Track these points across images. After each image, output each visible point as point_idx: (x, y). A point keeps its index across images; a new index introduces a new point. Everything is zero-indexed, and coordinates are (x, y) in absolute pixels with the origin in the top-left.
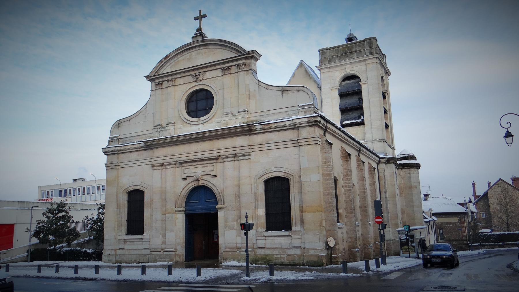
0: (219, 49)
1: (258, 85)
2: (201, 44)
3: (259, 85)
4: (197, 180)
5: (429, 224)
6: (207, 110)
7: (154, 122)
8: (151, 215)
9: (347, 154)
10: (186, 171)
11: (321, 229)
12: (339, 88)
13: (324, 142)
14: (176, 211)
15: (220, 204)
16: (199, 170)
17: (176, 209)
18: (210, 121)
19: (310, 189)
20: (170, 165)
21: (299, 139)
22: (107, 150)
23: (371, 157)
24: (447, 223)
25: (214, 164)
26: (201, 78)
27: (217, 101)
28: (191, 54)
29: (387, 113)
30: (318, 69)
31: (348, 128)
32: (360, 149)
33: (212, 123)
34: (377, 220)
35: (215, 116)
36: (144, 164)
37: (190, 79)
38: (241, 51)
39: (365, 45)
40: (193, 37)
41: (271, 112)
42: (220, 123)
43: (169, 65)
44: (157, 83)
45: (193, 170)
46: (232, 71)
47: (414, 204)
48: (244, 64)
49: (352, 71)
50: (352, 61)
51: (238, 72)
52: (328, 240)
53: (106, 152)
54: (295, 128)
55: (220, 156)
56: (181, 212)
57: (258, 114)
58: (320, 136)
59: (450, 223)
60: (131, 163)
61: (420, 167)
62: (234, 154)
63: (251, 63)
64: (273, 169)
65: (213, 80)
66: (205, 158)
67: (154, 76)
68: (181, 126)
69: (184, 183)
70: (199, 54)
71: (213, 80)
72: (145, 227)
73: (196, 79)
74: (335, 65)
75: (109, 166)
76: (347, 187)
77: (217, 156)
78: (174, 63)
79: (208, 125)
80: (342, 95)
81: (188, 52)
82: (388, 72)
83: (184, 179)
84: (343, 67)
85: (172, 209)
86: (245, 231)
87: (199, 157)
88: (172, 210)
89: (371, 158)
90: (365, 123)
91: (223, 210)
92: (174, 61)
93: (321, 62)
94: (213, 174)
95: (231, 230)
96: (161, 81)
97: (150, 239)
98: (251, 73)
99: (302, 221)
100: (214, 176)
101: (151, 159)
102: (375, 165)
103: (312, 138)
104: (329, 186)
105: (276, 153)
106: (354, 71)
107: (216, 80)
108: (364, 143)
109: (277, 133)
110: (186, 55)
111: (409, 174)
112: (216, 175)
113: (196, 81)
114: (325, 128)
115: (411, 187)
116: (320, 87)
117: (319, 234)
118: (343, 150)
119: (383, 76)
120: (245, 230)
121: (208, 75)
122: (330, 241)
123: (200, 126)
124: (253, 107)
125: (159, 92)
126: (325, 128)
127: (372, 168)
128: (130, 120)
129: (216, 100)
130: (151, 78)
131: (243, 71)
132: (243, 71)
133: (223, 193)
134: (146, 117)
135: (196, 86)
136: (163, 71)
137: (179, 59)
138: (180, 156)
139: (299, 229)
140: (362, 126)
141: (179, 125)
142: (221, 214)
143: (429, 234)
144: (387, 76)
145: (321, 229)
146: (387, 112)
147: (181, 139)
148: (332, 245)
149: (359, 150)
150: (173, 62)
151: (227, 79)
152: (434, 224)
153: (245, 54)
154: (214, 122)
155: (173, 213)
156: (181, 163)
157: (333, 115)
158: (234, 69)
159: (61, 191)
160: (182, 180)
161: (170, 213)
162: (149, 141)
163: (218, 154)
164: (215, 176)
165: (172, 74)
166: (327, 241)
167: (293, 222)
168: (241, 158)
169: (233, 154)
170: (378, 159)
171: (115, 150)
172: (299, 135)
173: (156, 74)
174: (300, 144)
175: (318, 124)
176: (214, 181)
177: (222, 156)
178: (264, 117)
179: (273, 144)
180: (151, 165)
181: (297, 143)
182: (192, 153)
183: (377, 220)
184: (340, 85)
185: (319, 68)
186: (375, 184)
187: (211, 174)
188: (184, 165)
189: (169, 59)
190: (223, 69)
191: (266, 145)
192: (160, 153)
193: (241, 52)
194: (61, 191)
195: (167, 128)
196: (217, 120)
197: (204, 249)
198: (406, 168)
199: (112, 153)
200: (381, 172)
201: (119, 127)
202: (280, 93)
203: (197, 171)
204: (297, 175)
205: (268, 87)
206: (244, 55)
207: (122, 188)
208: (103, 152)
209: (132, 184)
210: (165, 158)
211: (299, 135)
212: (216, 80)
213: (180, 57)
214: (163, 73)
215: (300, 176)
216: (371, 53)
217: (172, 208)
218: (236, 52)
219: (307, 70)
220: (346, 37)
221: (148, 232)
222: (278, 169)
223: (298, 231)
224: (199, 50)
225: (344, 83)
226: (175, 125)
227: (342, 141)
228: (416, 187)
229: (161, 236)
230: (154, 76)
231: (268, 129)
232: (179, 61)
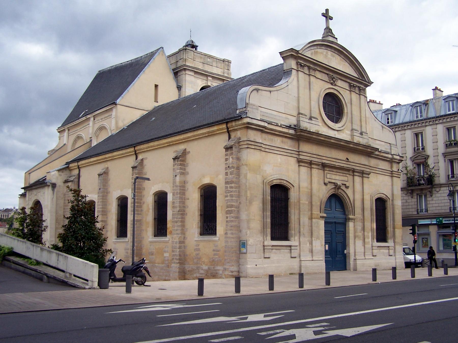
0: (347, 63)
2: (341, 49)
10: (328, 176)
15: (351, 215)
16: (338, 177)
25: (348, 175)
37: (326, 78)
45: (333, 177)
65: (343, 91)
66: (346, 167)
70: (333, 56)
73: (332, 81)
78: (313, 51)
85: (318, 214)
91: (353, 221)
112: (349, 187)
121: (339, 83)
123: (336, 132)
142: (351, 225)
153: (367, 81)
174: (394, 175)
177: (356, 169)
192: (306, 148)
202: (381, 128)
206: (367, 82)
209: (277, 176)
224: (334, 52)
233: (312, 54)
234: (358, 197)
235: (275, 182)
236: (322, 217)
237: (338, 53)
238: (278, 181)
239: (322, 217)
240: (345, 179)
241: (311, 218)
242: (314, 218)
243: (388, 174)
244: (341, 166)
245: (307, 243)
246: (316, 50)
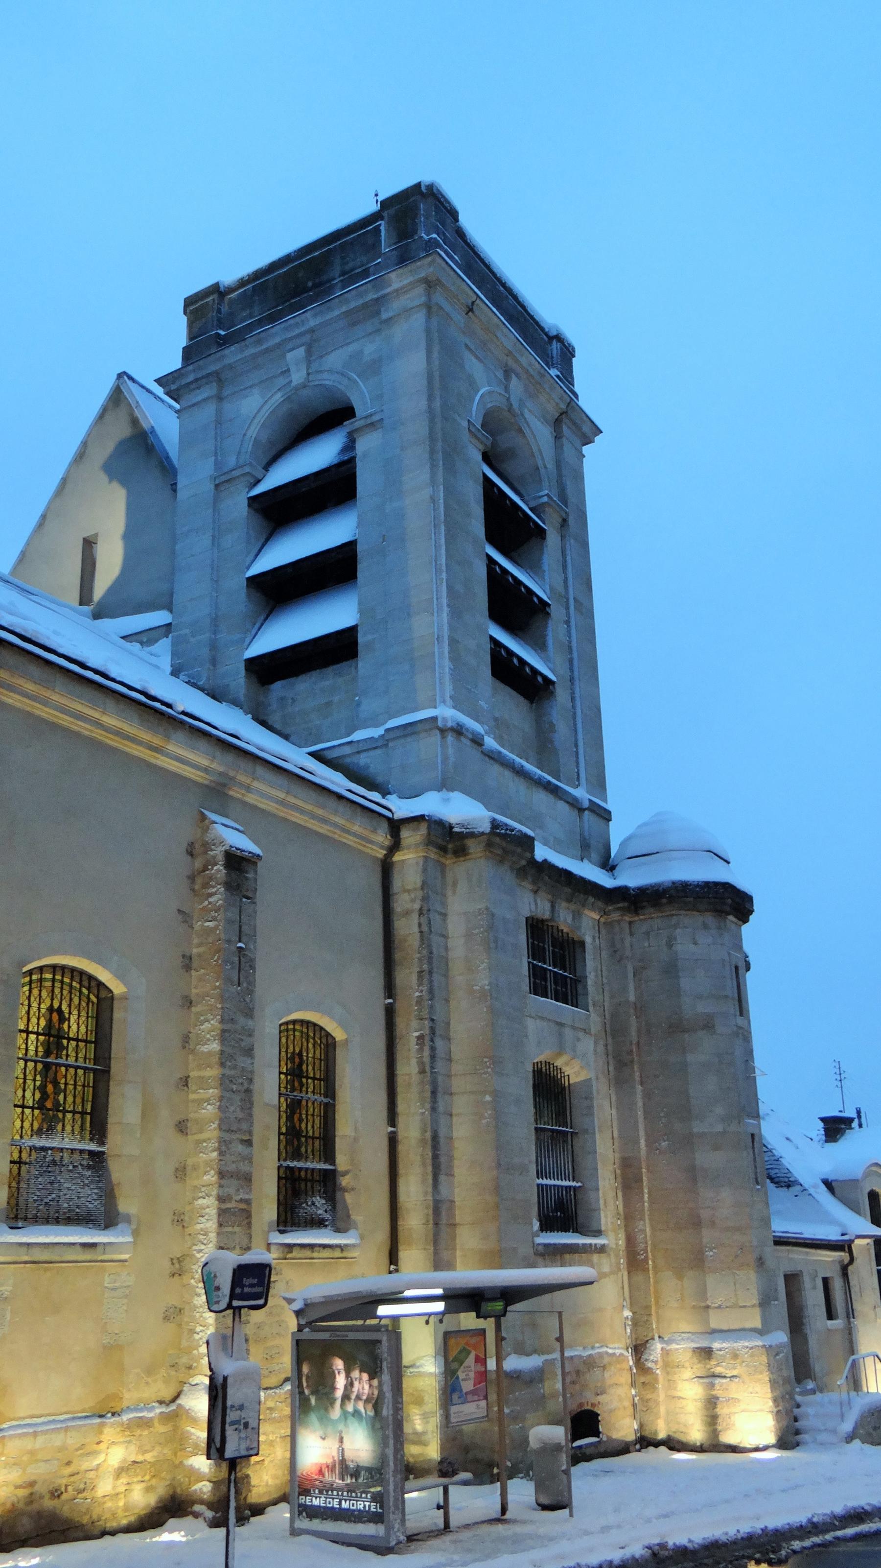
31: (292, 680)
47: (698, 1127)
108: (347, 750)
111: (670, 946)
185: (173, 387)
200: (407, 913)
219: (137, 413)
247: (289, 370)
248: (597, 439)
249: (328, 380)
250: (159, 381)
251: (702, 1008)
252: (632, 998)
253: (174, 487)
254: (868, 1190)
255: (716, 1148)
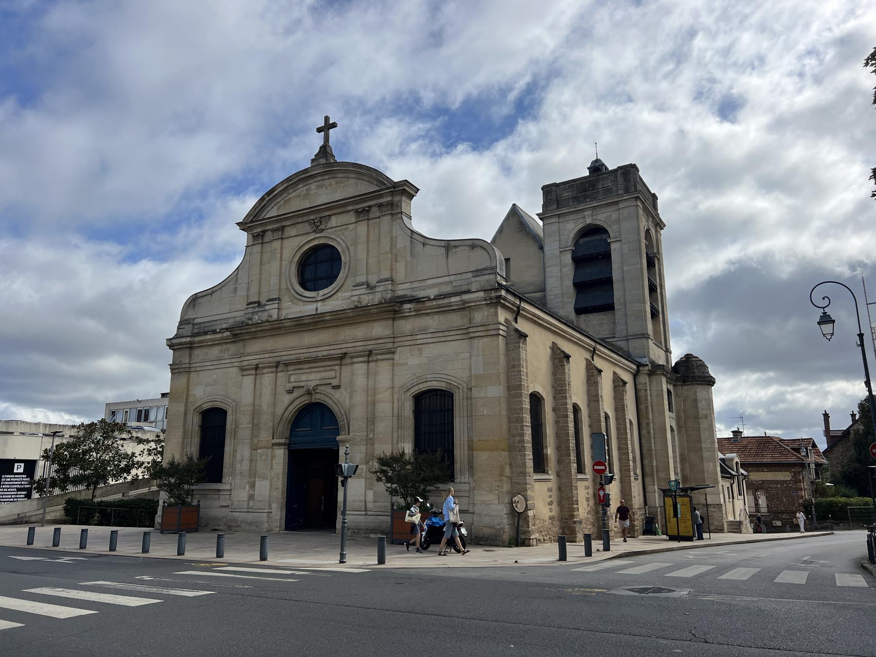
1: (410, 239)
3: (411, 238)
4: (309, 393)
5: (732, 482)
6: (331, 278)
7: (248, 296)
8: (235, 451)
9: (562, 355)
11: (501, 480)
12: (574, 249)
13: (512, 333)
14: (273, 445)
15: (343, 433)
16: (312, 376)
17: (274, 441)
18: (335, 296)
19: (485, 411)
20: (269, 367)
21: (470, 326)
22: (174, 341)
23: (619, 362)
24: (772, 482)
25: (337, 368)
26: (322, 227)
27: (345, 263)
28: (310, 187)
29: (657, 292)
30: (540, 219)
31: (588, 315)
32: (594, 349)
33: (337, 299)
34: (596, 467)
35: (343, 289)
36: (229, 365)
38: (385, 182)
39: (618, 176)
40: (313, 160)
41: (429, 282)
42: (349, 300)
43: (275, 205)
44: (255, 235)
45: (304, 377)
46: (371, 215)
48: (391, 204)
49: (596, 221)
50: (594, 205)
51: (379, 217)
52: (513, 501)
53: (171, 344)
54: (464, 308)
55: (346, 354)
56: (281, 447)
57: (407, 286)
58: (505, 322)
59: (777, 482)
60: (209, 363)
61: (714, 383)
62: (367, 351)
63: (400, 201)
64: (428, 376)
65: (341, 230)
66: (322, 356)
67: (251, 222)
68: (290, 305)
69: (287, 399)
70: (322, 187)
71: (341, 230)
72: (225, 470)
74: (567, 211)
75: (176, 369)
76: (562, 410)
77: (342, 354)
78: (282, 202)
79: (330, 302)
80: (579, 261)
81: (305, 184)
82: (659, 223)
83: (290, 392)
84: (581, 215)
85: (268, 441)
86: (343, 479)
87: (314, 355)
88: (268, 442)
89: (620, 364)
90: (616, 307)
92: (283, 199)
93: (545, 206)
94: (335, 382)
95: (358, 478)
96: (262, 232)
97: (230, 490)
98: (400, 218)
99: (471, 466)
100: (336, 386)
101: (240, 357)
102: (627, 377)
103: (490, 326)
104: (518, 407)
105: (432, 351)
106: (598, 221)
107: (345, 229)
109: (436, 317)
110: (302, 189)
113: (314, 231)
114: (515, 309)
115: (698, 415)
116: (543, 248)
117: (497, 490)
118: (554, 348)
119: (650, 229)
120: (342, 475)
122: (518, 502)
123: (319, 304)
124: (400, 274)
125: (258, 248)
126: (515, 309)
127: (620, 381)
128: (211, 295)
129: (344, 262)
130: (247, 226)
131: (387, 214)
132: (387, 214)
133: (348, 415)
134: (236, 288)
135: (314, 239)
136: (265, 215)
137: (292, 195)
138: (284, 353)
139: (466, 480)
140: (610, 312)
141: (286, 303)
143: (733, 498)
144: (658, 229)
145: (501, 480)
146: (657, 289)
147: (286, 324)
148: (520, 508)
149: (592, 349)
150: (281, 201)
151: (362, 228)
152: (744, 481)
154: (340, 299)
155: (268, 448)
156: (286, 365)
157: (562, 293)
158: (375, 212)
159: (140, 412)
160: (285, 393)
161: (265, 447)
162: (237, 329)
163: (343, 351)
164: (337, 387)
165: (279, 219)
166: (512, 502)
167: (457, 466)
168: (379, 357)
169: (366, 351)
170: (635, 367)
171: (185, 342)
172: (470, 320)
173: (254, 219)
174: (472, 335)
175: (502, 301)
176: (337, 394)
178: (417, 291)
179: (430, 335)
180: (239, 367)
181: (467, 333)
182: (303, 349)
183: (596, 467)
184: (576, 243)
185: (542, 217)
186: (626, 409)
187: (331, 384)
188: (291, 368)
189: (276, 195)
190: (357, 212)
191: (418, 337)
193: (385, 184)
194: (140, 412)
195: (267, 307)
196: (344, 294)
197: (322, 510)
198: (688, 385)
199: (181, 346)
201: (194, 306)
202: (443, 251)
203: (311, 378)
204: (465, 385)
205: (425, 241)
206: (389, 188)
207: (194, 404)
208: (168, 345)
209: (209, 398)
210: (262, 356)
211: (470, 320)
212: (345, 229)
213: (292, 192)
214: (266, 217)
215: (471, 389)
216: (627, 191)
217: (267, 439)
218: (379, 184)
220: (589, 166)
221: (229, 478)
222: (436, 376)
223: (464, 483)
224: (321, 180)
225: (582, 241)
226: (280, 302)
227: (554, 333)
228: (706, 417)
229: (247, 487)
230: (251, 222)
231: (422, 310)
232: (290, 199)
233: (278, 209)
234: (360, 398)
235: (206, 406)
236: (279, 444)
237: (330, 176)
238: (210, 404)
239: (279, 444)
240: (332, 374)
241: (254, 448)
242: (261, 448)
243: (459, 337)
244: (312, 357)
245: (246, 487)
246: (288, 197)
247: (585, 217)
248: (665, 228)
249: (599, 223)
250: (537, 215)
251: (705, 412)
252: (683, 408)
253: (541, 248)
254: (735, 462)
255: (708, 451)
